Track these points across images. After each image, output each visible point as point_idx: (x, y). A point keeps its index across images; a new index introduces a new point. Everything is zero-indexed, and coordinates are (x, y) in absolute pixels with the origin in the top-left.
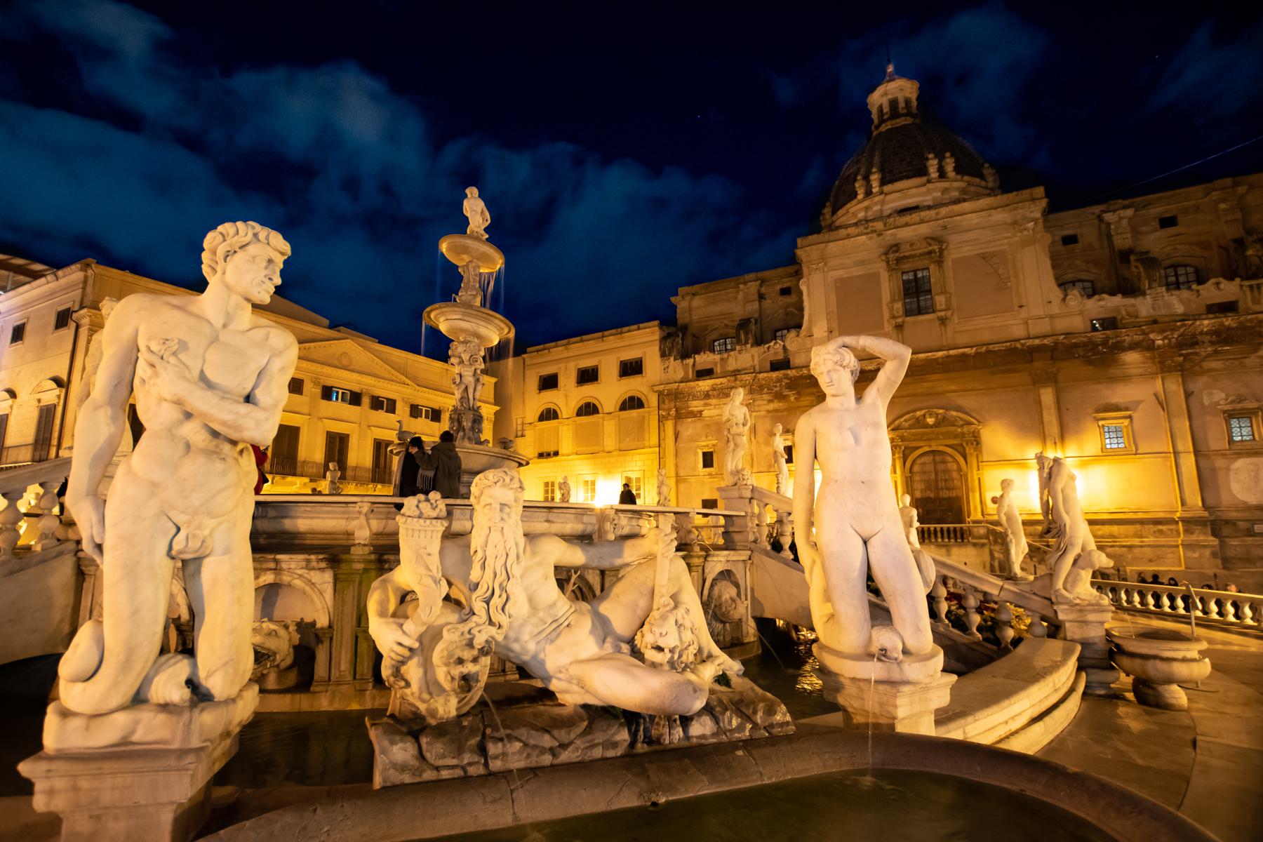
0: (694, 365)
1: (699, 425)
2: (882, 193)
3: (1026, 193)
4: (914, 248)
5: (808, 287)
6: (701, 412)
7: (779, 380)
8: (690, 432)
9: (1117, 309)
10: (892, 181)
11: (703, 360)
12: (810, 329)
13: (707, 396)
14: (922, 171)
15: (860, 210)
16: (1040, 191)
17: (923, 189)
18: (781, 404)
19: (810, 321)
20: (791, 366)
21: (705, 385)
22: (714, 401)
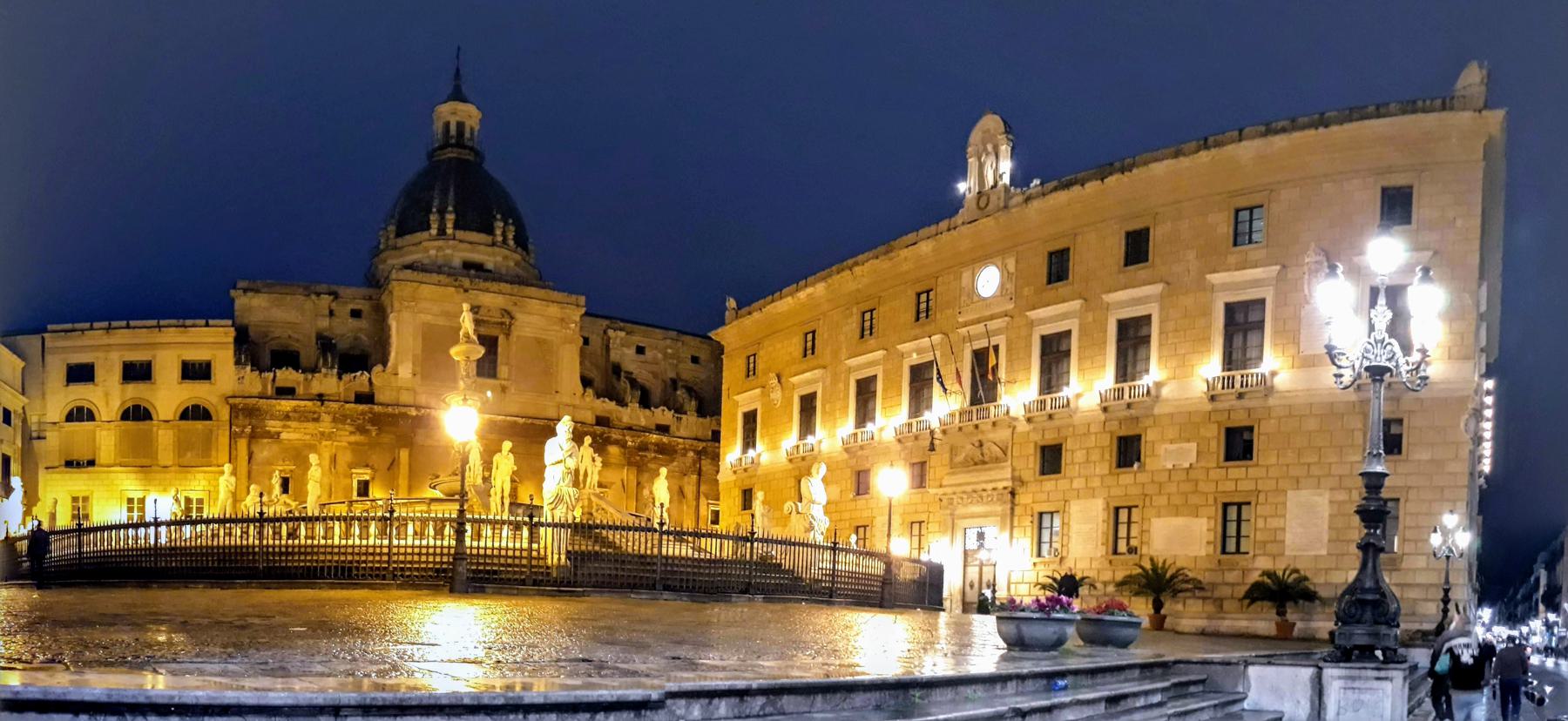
0: (274, 380)
1: (275, 448)
2: (454, 239)
3: (574, 297)
4: (491, 313)
5: (398, 322)
6: (278, 434)
7: (363, 413)
8: (265, 453)
9: (610, 412)
10: (465, 228)
11: (283, 377)
12: (395, 367)
13: (287, 417)
14: (489, 231)
15: (433, 248)
16: (582, 299)
17: (490, 249)
18: (362, 437)
19: (396, 358)
20: (376, 401)
21: (286, 405)
22: (293, 424)
